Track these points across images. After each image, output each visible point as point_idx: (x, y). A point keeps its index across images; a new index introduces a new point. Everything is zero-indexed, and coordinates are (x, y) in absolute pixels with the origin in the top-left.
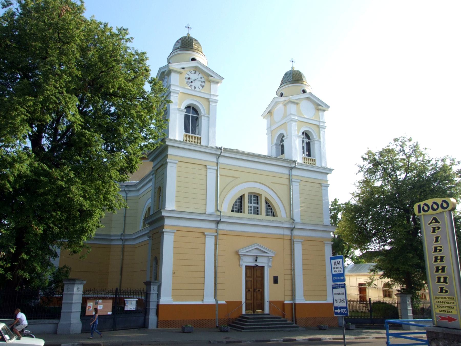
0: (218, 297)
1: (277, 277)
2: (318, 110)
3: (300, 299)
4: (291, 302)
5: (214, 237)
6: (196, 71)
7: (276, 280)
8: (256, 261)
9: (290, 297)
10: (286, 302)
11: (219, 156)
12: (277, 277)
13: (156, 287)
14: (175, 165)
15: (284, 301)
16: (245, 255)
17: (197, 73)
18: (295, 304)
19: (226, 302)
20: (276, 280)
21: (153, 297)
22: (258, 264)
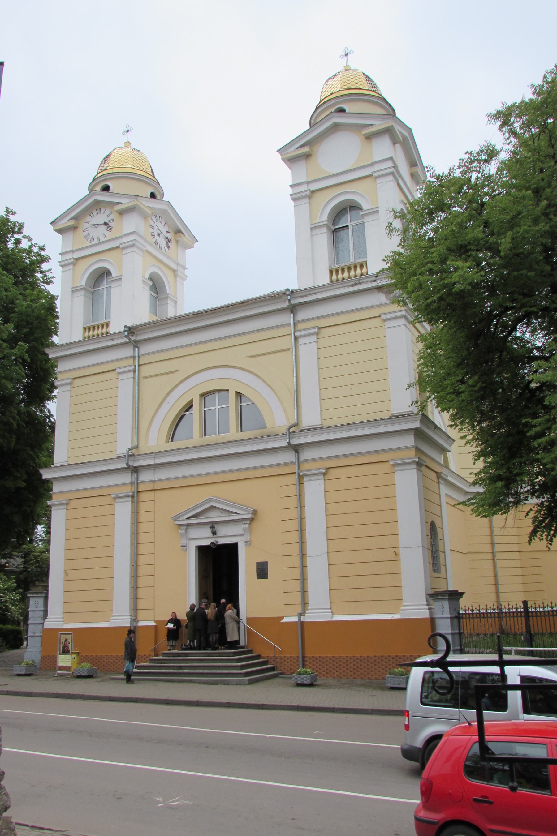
0: (141, 614)
1: (266, 563)
2: (369, 137)
3: (319, 612)
4: (295, 619)
5: (130, 499)
6: (100, 209)
7: (262, 571)
8: (214, 533)
9: (299, 609)
10: (285, 620)
11: (136, 344)
12: (266, 563)
13: (41, 601)
14: (68, 388)
15: (283, 618)
16: (188, 525)
17: (102, 210)
18: (302, 624)
19: (155, 622)
20: (262, 571)
21: (34, 617)
22: (222, 541)
